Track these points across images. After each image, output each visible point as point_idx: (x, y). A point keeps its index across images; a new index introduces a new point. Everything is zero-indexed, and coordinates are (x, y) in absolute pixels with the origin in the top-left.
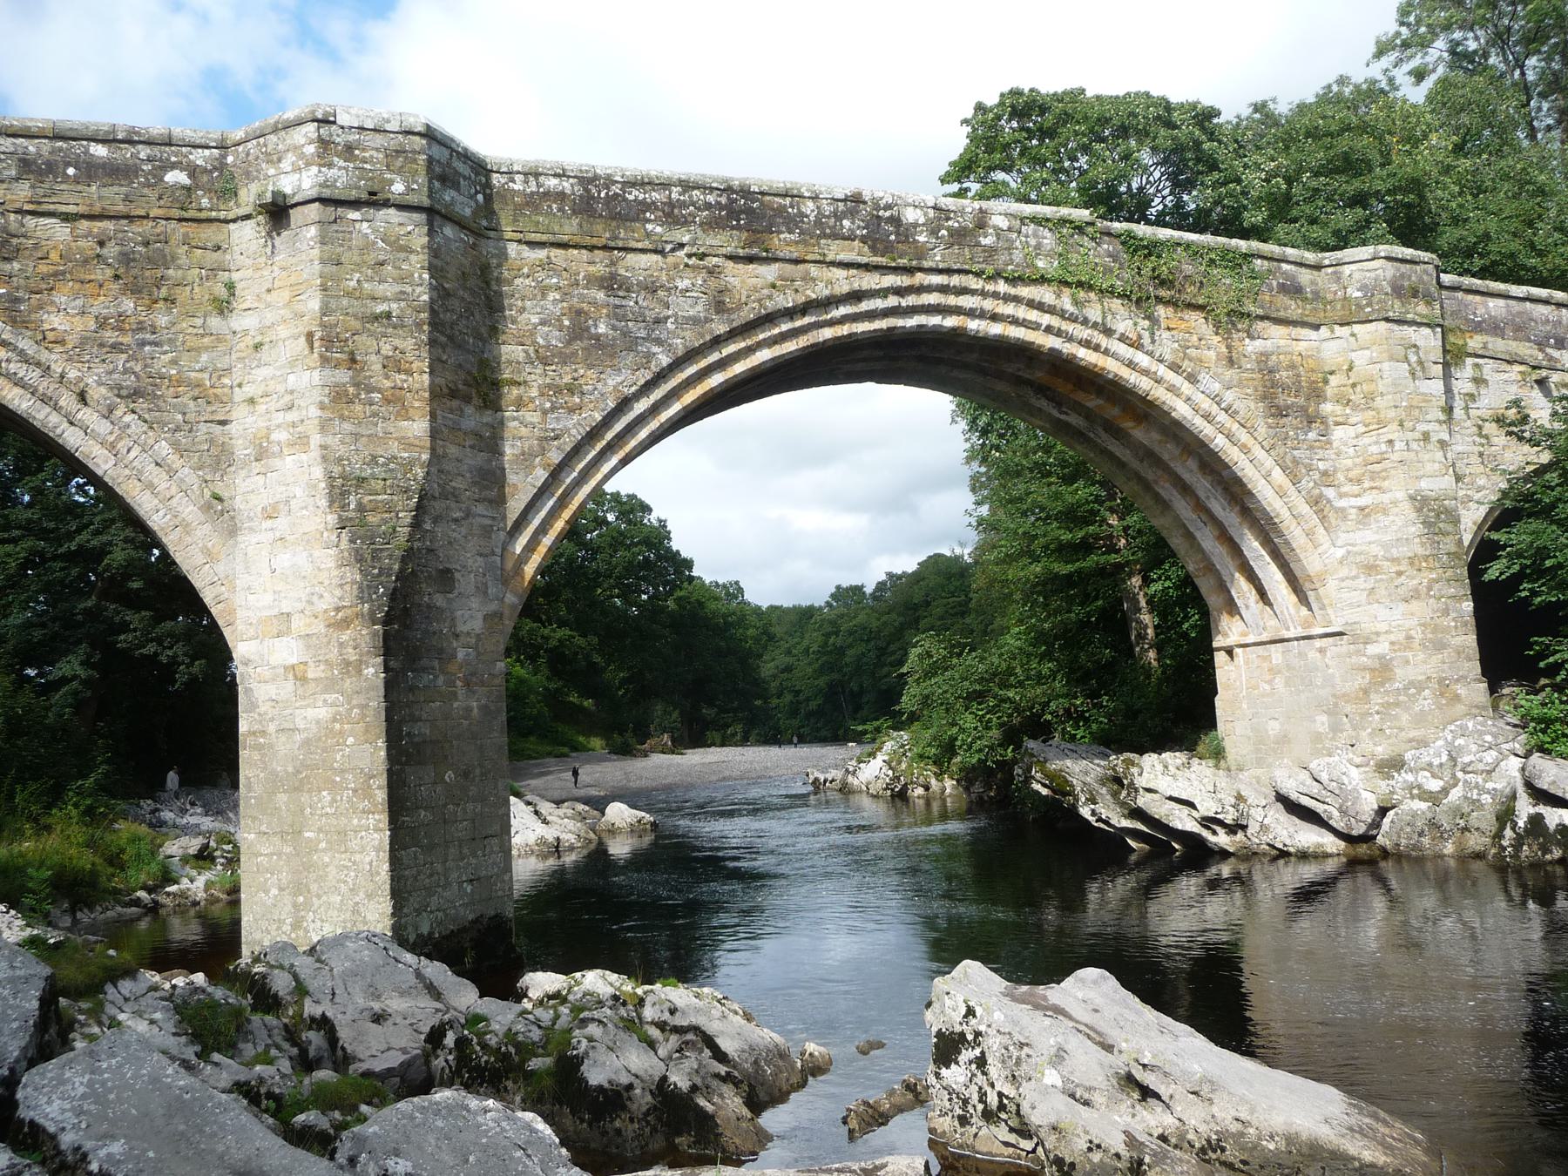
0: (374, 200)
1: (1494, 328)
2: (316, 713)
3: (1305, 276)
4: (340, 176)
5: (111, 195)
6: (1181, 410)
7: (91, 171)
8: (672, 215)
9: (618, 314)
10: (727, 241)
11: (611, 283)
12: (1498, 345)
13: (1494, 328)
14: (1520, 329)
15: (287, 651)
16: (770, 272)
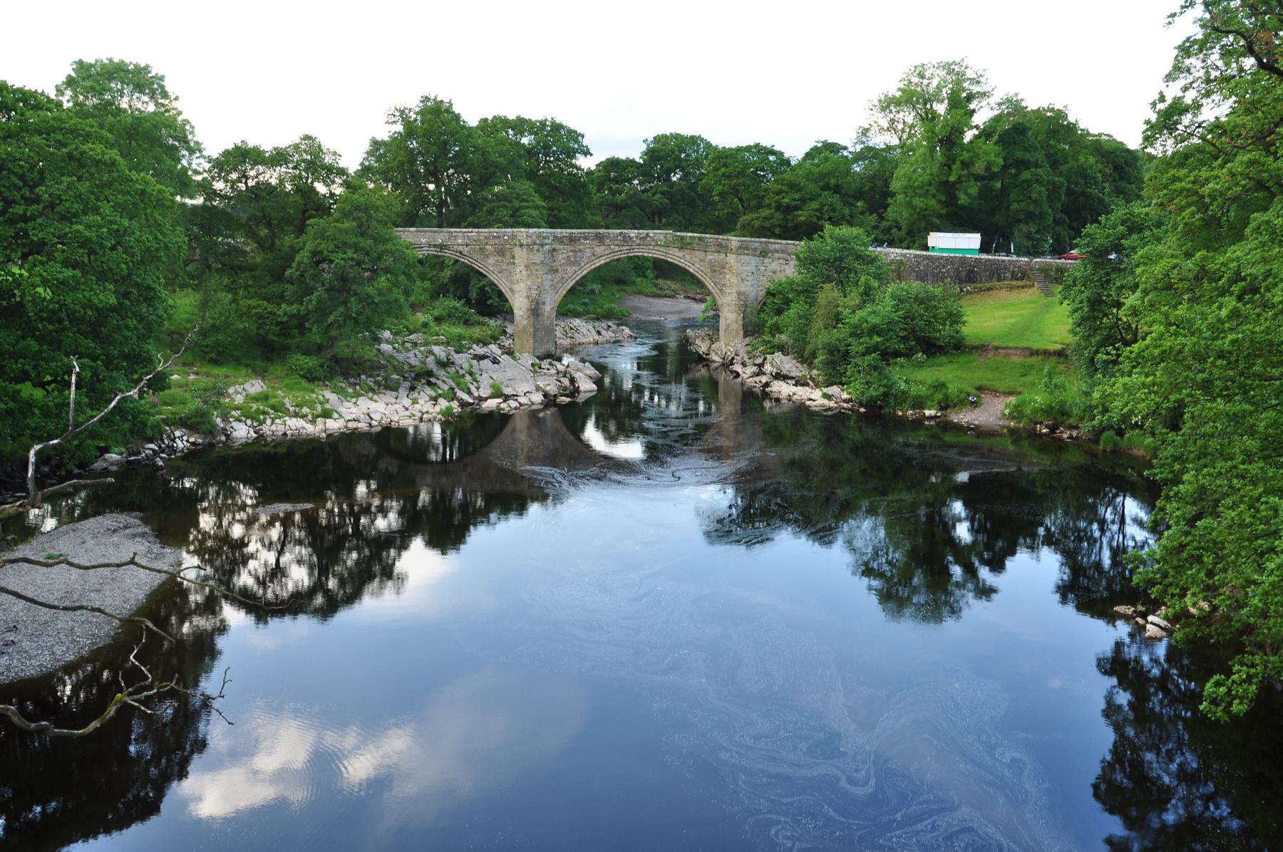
0: (535, 244)
1: (776, 251)
2: (525, 322)
3: (724, 242)
4: (529, 240)
5: (497, 241)
6: (691, 270)
7: (494, 237)
8: (586, 239)
9: (575, 257)
10: (595, 242)
11: (574, 251)
12: (777, 255)
13: (776, 251)
14: (783, 252)
15: (521, 313)
16: (603, 248)
